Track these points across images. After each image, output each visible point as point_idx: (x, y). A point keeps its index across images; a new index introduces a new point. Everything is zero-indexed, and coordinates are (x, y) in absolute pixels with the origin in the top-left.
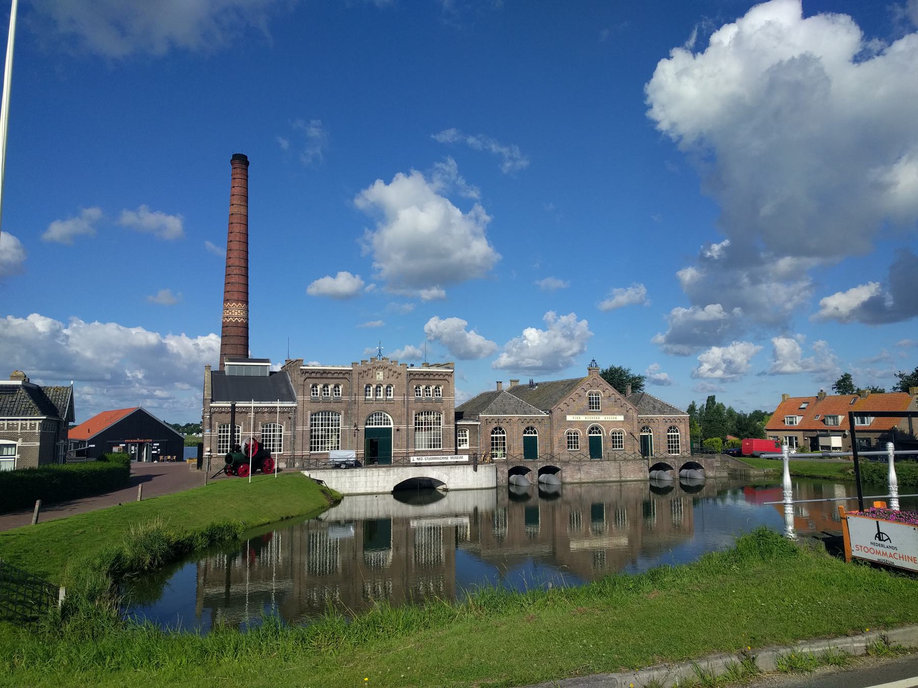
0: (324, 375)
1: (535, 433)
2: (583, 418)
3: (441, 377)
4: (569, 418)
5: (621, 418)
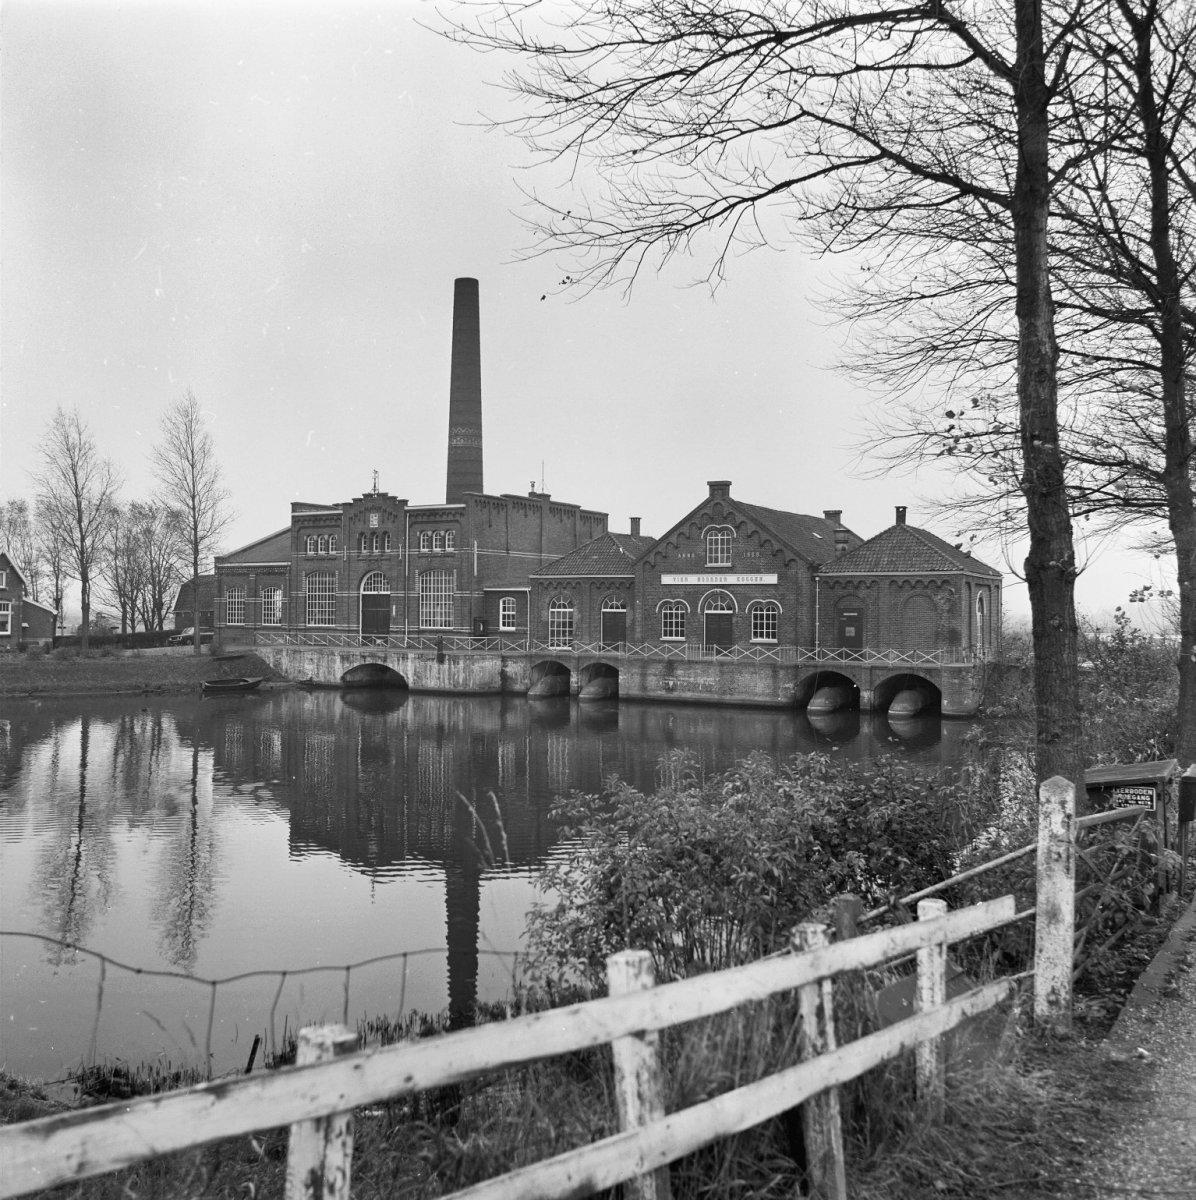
0: (317, 523)
1: (623, 607)
2: (692, 579)
3: (451, 518)
4: (667, 579)
5: (772, 579)
